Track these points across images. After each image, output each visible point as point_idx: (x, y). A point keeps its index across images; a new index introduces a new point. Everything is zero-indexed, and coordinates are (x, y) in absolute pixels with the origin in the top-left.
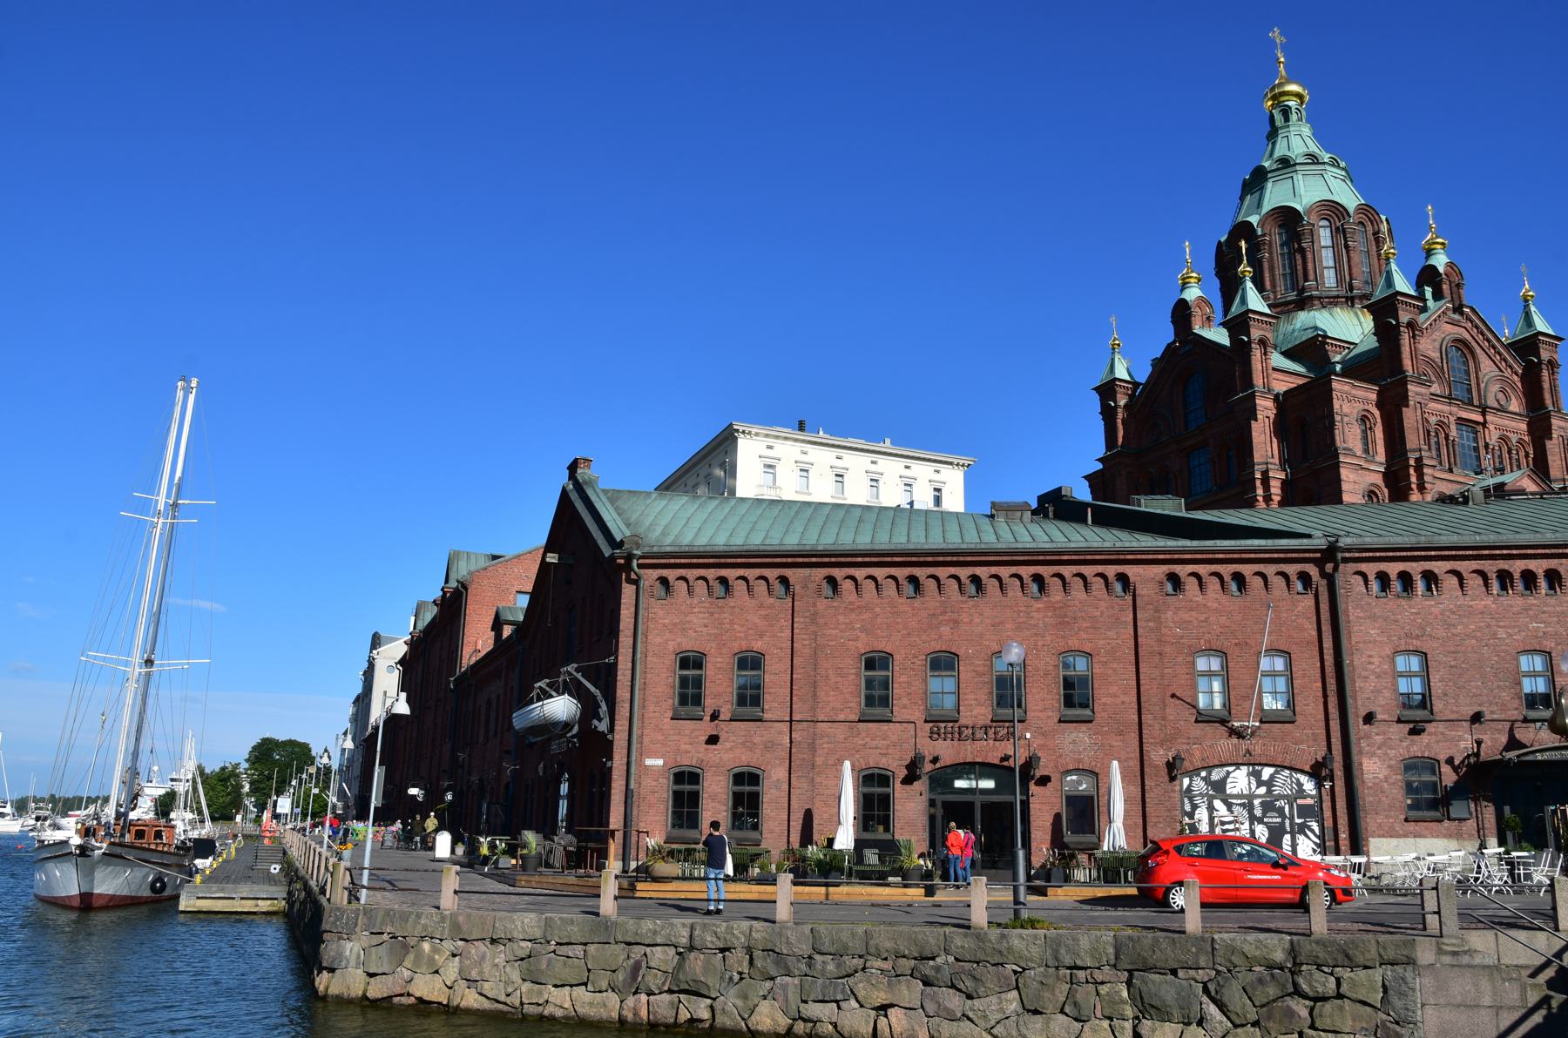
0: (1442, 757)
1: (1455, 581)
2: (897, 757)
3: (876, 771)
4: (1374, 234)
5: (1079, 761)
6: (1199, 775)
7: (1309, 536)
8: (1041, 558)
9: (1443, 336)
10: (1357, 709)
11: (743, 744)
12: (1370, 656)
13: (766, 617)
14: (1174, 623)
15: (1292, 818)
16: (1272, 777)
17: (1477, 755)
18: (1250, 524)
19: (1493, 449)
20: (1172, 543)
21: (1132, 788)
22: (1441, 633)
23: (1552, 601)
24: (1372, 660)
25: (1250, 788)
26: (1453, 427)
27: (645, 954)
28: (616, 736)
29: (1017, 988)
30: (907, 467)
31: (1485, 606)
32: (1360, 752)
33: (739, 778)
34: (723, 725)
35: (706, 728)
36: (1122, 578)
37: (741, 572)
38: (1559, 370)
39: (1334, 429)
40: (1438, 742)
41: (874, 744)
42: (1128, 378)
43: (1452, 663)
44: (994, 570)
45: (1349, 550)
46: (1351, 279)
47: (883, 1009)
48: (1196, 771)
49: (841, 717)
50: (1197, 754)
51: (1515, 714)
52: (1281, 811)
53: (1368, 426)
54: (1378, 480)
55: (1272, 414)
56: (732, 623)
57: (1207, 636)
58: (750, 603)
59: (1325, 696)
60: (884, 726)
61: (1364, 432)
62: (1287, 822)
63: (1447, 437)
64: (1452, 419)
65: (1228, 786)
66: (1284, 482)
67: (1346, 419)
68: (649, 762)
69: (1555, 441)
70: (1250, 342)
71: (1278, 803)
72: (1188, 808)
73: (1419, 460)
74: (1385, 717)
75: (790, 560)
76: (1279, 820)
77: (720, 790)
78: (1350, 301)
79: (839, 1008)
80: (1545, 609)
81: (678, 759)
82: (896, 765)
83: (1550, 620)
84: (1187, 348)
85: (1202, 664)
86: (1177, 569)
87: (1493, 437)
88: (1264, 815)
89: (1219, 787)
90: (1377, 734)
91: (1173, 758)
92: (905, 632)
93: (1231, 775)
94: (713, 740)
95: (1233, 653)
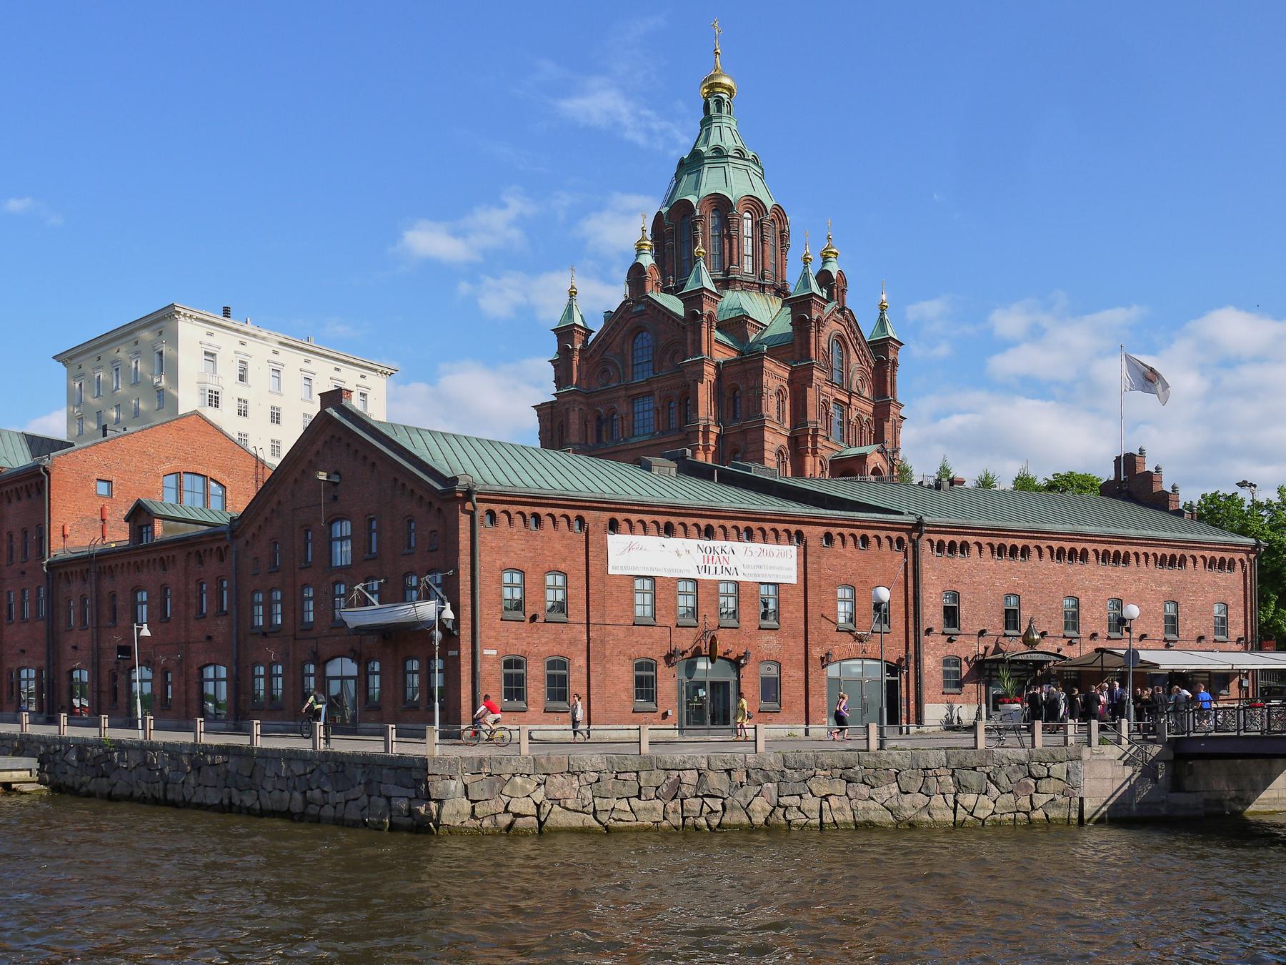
0: (963, 657)
1: (976, 548)
2: (659, 650)
3: (645, 660)
5: (770, 655)
7: (902, 513)
8: (753, 516)
10: (924, 627)
12: (931, 593)
18: (855, 499)
20: (823, 512)
21: (800, 673)
22: (968, 581)
23: (1023, 564)
26: (832, 405)
27: (679, 776)
28: (462, 632)
29: (897, 781)
30: (337, 369)
33: (551, 665)
37: (550, 510)
38: (898, 369)
39: (761, 399)
41: (643, 641)
42: (582, 325)
44: (722, 522)
45: (928, 525)
46: (763, 270)
47: (825, 798)
49: (622, 622)
50: (837, 651)
51: (1000, 632)
54: (784, 441)
55: (713, 378)
56: (542, 548)
57: (845, 576)
58: (556, 534)
59: (907, 617)
61: (779, 403)
63: (827, 414)
64: (832, 399)
66: (718, 436)
68: (486, 652)
69: (890, 423)
70: (702, 316)
73: (816, 430)
75: (587, 504)
77: (539, 673)
78: (762, 288)
79: (801, 798)
82: (657, 654)
84: (639, 308)
86: (832, 529)
87: (853, 415)
95: (859, 587)
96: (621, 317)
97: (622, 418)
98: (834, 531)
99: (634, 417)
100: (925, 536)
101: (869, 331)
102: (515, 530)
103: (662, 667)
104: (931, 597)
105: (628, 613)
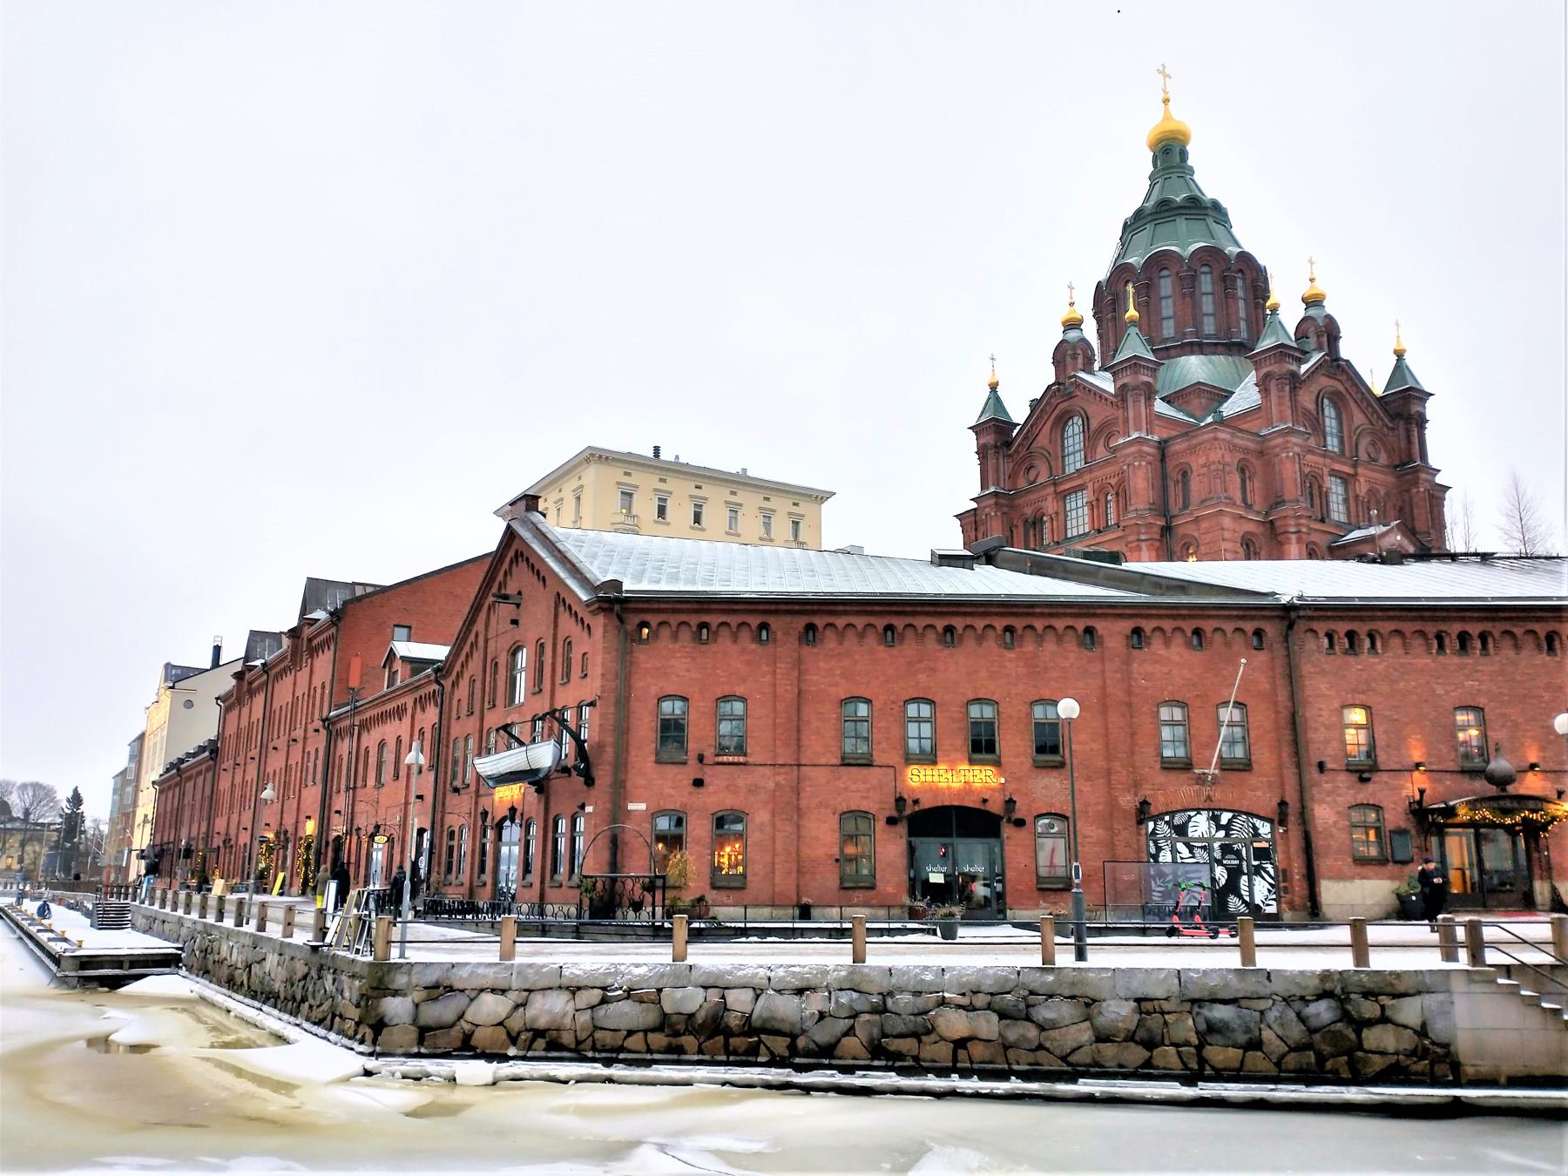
4: (1252, 281)
5: (1051, 805)
6: (1163, 819)
9: (1320, 388)
11: (727, 787)
12: (1320, 709)
13: (748, 663)
14: (1140, 674)
15: (1248, 861)
16: (1230, 821)
17: (1420, 802)
19: (1363, 502)
24: (1322, 713)
25: (1210, 832)
31: (1426, 664)
32: (1312, 800)
34: (706, 769)
35: (692, 771)
36: (1089, 631)
38: (1427, 425)
40: (1382, 790)
41: (854, 787)
43: (1396, 717)
48: (1159, 817)
49: (823, 761)
50: (1161, 799)
52: (1238, 854)
53: (1247, 475)
58: (733, 649)
60: (865, 771)
61: (1243, 482)
62: (1244, 864)
64: (1326, 471)
65: (1190, 830)
67: (1227, 468)
68: (631, 807)
71: (1236, 846)
72: (1153, 850)
74: (1334, 766)
76: (1237, 862)
79: (920, 1041)
80: (1479, 668)
81: (662, 803)
83: (1484, 678)
85: (1165, 713)
88: (1223, 858)
89: (1181, 830)
90: (1327, 782)
91: (1141, 803)
92: (882, 678)
93: (1193, 819)
94: (698, 783)
96: (1048, 403)
97: (1052, 519)
98: (1148, 626)
99: (1066, 516)
100: (1301, 626)
101: (1378, 383)
102: (678, 645)
103: (881, 825)
104: (1320, 716)
105: (832, 749)
